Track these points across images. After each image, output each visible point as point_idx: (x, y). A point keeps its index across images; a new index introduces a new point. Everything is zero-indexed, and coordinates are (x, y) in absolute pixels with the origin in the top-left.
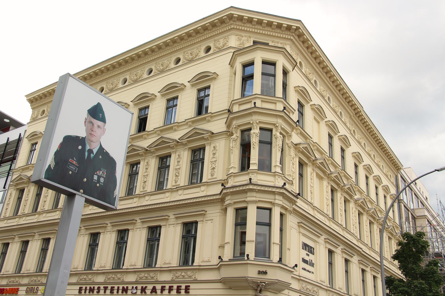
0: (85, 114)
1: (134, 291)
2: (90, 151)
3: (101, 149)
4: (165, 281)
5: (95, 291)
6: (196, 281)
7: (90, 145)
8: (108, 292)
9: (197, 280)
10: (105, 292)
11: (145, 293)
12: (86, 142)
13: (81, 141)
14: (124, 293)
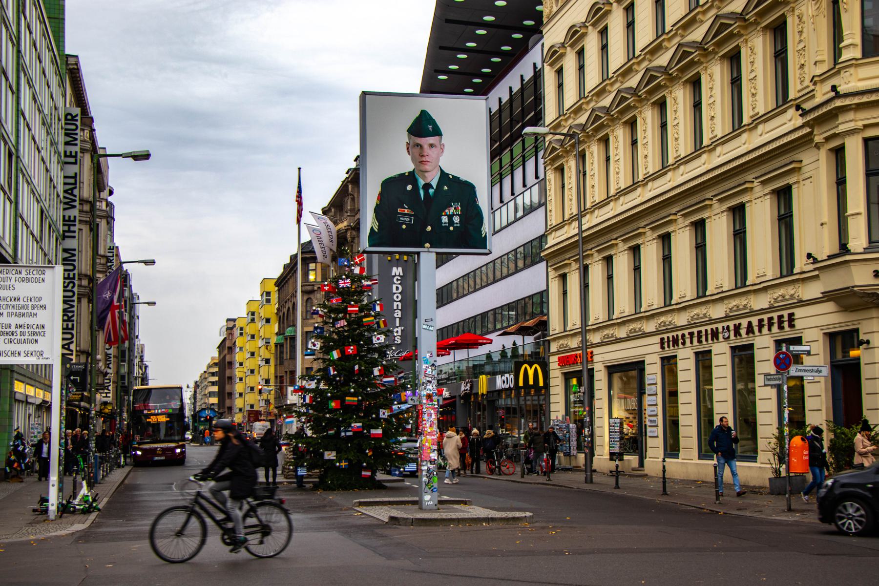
0: (405, 138)
1: (726, 335)
2: (427, 186)
3: (444, 175)
4: (762, 309)
5: (680, 341)
6: (802, 303)
7: (424, 178)
8: (695, 340)
9: (801, 301)
10: (691, 342)
11: (740, 335)
12: (417, 176)
13: (411, 177)
14: (715, 341)
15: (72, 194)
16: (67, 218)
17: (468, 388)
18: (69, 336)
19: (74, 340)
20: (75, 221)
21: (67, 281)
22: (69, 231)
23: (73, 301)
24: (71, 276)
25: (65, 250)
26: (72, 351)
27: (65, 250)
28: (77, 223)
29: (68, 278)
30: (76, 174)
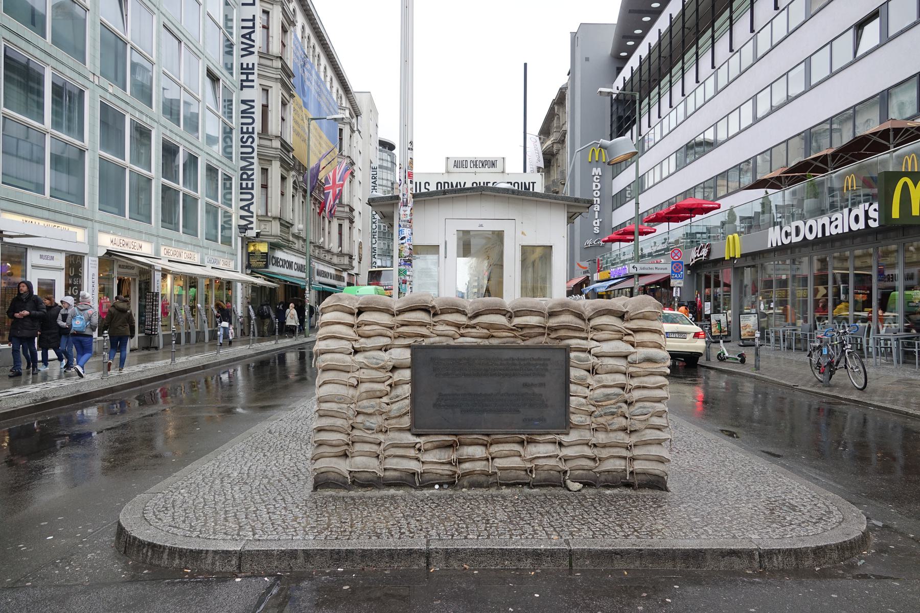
15: (250, 39)
16: (245, 66)
17: (704, 252)
18: (249, 197)
19: (254, 200)
20: (253, 69)
21: (246, 136)
22: (248, 80)
23: (253, 158)
24: (250, 130)
25: (243, 102)
26: (252, 213)
27: (243, 102)
28: (256, 71)
29: (248, 132)
30: (254, 16)
